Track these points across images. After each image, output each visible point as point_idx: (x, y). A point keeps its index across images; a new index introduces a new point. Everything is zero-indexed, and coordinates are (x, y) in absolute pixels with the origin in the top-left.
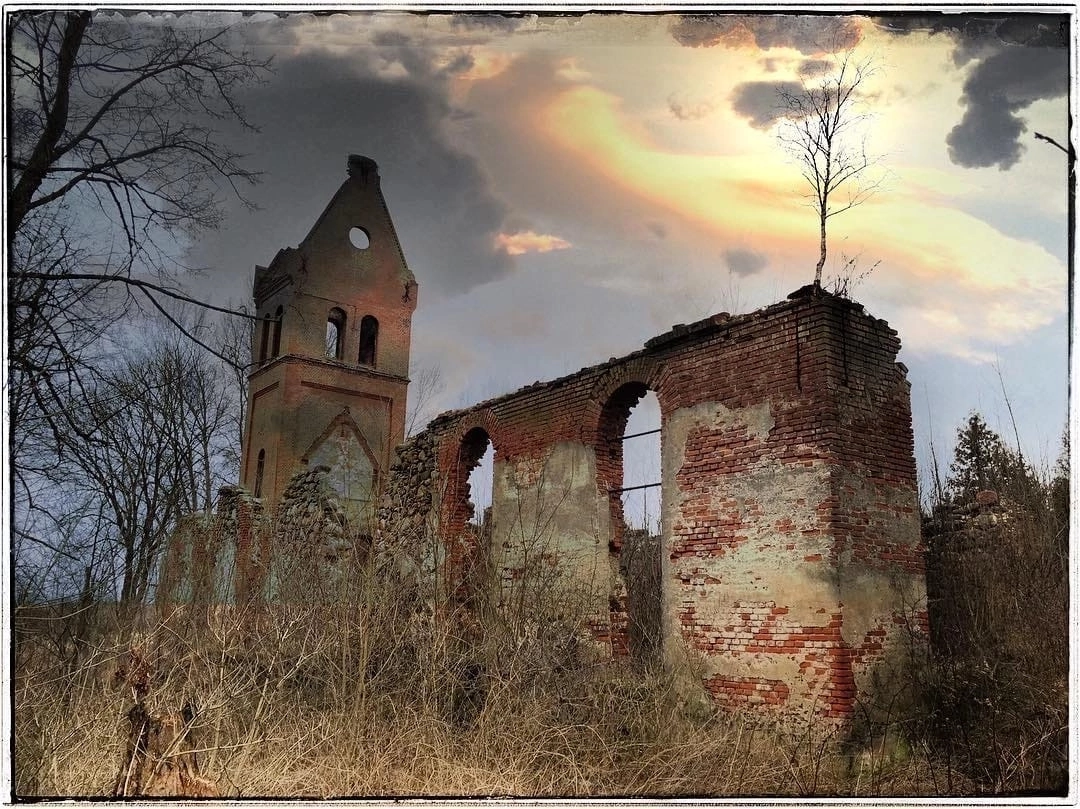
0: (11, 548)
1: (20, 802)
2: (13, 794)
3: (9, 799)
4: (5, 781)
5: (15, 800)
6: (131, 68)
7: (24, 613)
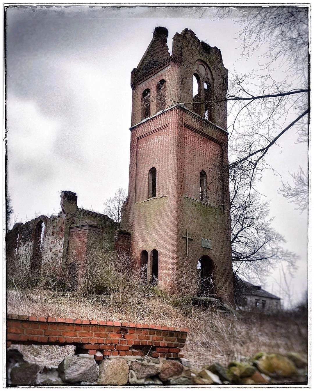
0: (6, 296)
1: (9, 386)
2: (7, 383)
3: (5, 386)
4: (4, 379)
5: (8, 386)
6: (261, 160)
7: (10, 350)
